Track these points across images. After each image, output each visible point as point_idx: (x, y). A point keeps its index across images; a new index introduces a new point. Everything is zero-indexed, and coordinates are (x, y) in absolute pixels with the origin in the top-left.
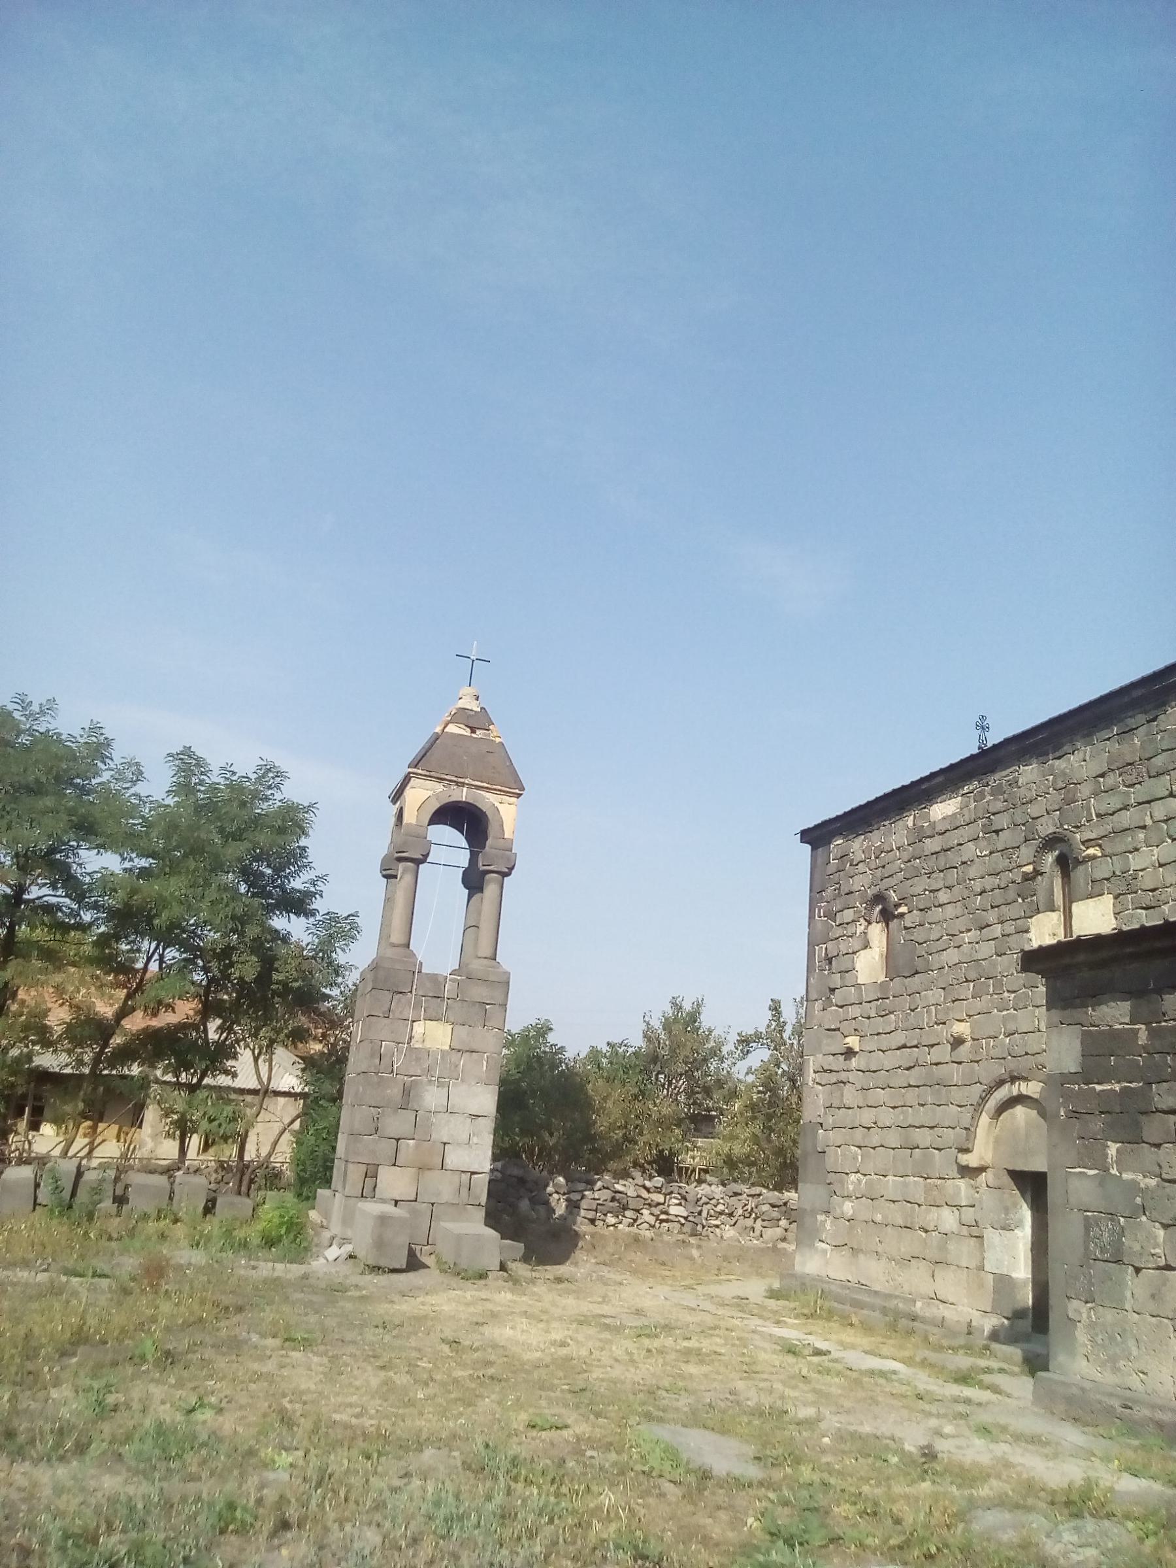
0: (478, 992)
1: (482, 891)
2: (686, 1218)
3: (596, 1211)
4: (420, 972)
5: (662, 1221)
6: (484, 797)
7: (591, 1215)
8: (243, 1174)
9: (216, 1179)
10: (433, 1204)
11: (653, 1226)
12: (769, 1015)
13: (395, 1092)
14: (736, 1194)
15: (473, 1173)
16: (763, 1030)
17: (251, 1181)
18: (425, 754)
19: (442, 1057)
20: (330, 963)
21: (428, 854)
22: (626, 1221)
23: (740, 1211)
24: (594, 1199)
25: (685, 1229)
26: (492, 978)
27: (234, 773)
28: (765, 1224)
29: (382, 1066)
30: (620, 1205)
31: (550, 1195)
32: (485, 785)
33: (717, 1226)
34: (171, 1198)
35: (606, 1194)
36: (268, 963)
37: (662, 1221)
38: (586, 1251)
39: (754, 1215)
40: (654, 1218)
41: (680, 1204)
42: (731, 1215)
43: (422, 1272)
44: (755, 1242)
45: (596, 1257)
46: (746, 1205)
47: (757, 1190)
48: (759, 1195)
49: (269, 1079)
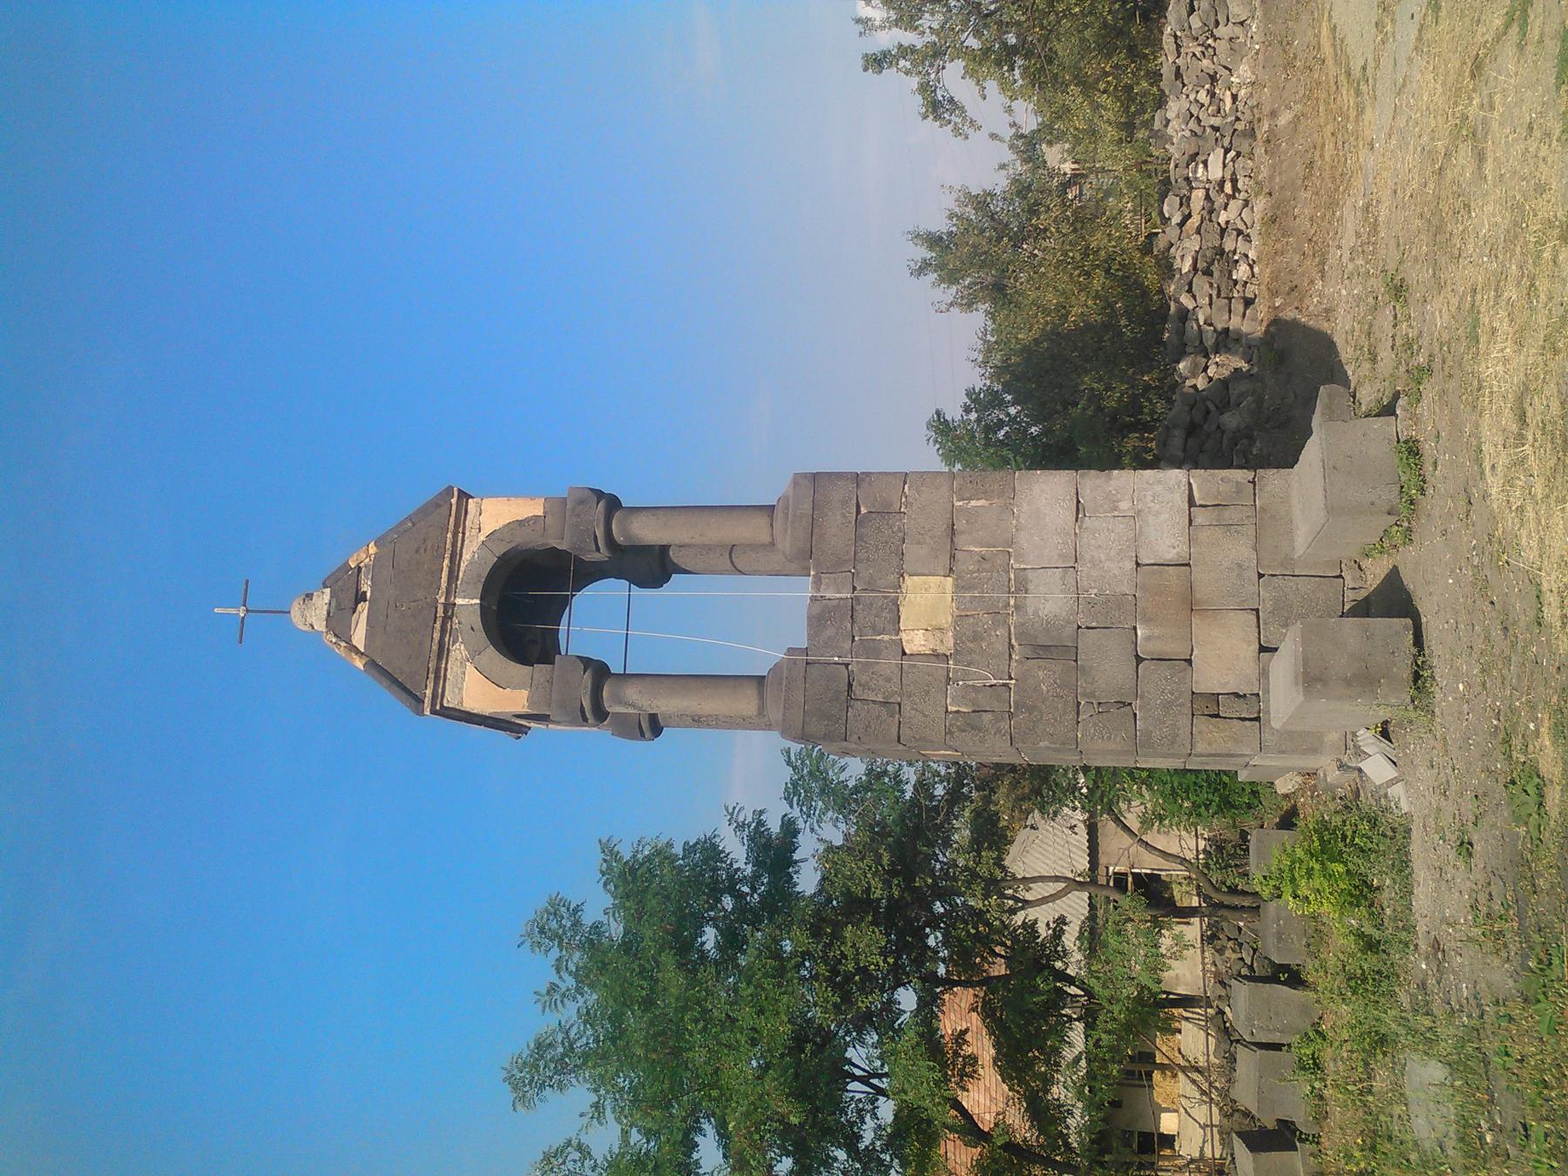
0: (837, 530)
1: (664, 549)
2: (1227, 151)
3: (1230, 299)
4: (806, 651)
5: (1235, 188)
6: (471, 563)
7: (1238, 306)
8: (1222, 906)
9: (1234, 951)
10: (1261, 576)
11: (1246, 203)
12: (889, 73)
13: (1045, 676)
14: (1178, 75)
15: (1191, 502)
16: (914, 82)
17: (1233, 890)
18: (395, 681)
19: (969, 587)
20: (867, 787)
21: (578, 657)
22: (1241, 246)
23: (1206, 62)
24: (1211, 304)
25: (1245, 148)
26: (807, 506)
27: (553, 988)
28: (1221, 19)
29: (997, 706)
30: (1217, 261)
31: (1211, 379)
32: (446, 562)
33: (1234, 97)
34: (1277, 1047)
35: (1200, 283)
36: (857, 906)
37: (1235, 188)
38: (1301, 300)
39: (1210, 41)
40: (1232, 202)
41: (1205, 163)
42: (1213, 78)
43: (1408, 579)
44: (1254, 29)
45: (1312, 282)
46: (1194, 55)
47: (1168, 42)
48: (1176, 37)
49: (1056, 879)
